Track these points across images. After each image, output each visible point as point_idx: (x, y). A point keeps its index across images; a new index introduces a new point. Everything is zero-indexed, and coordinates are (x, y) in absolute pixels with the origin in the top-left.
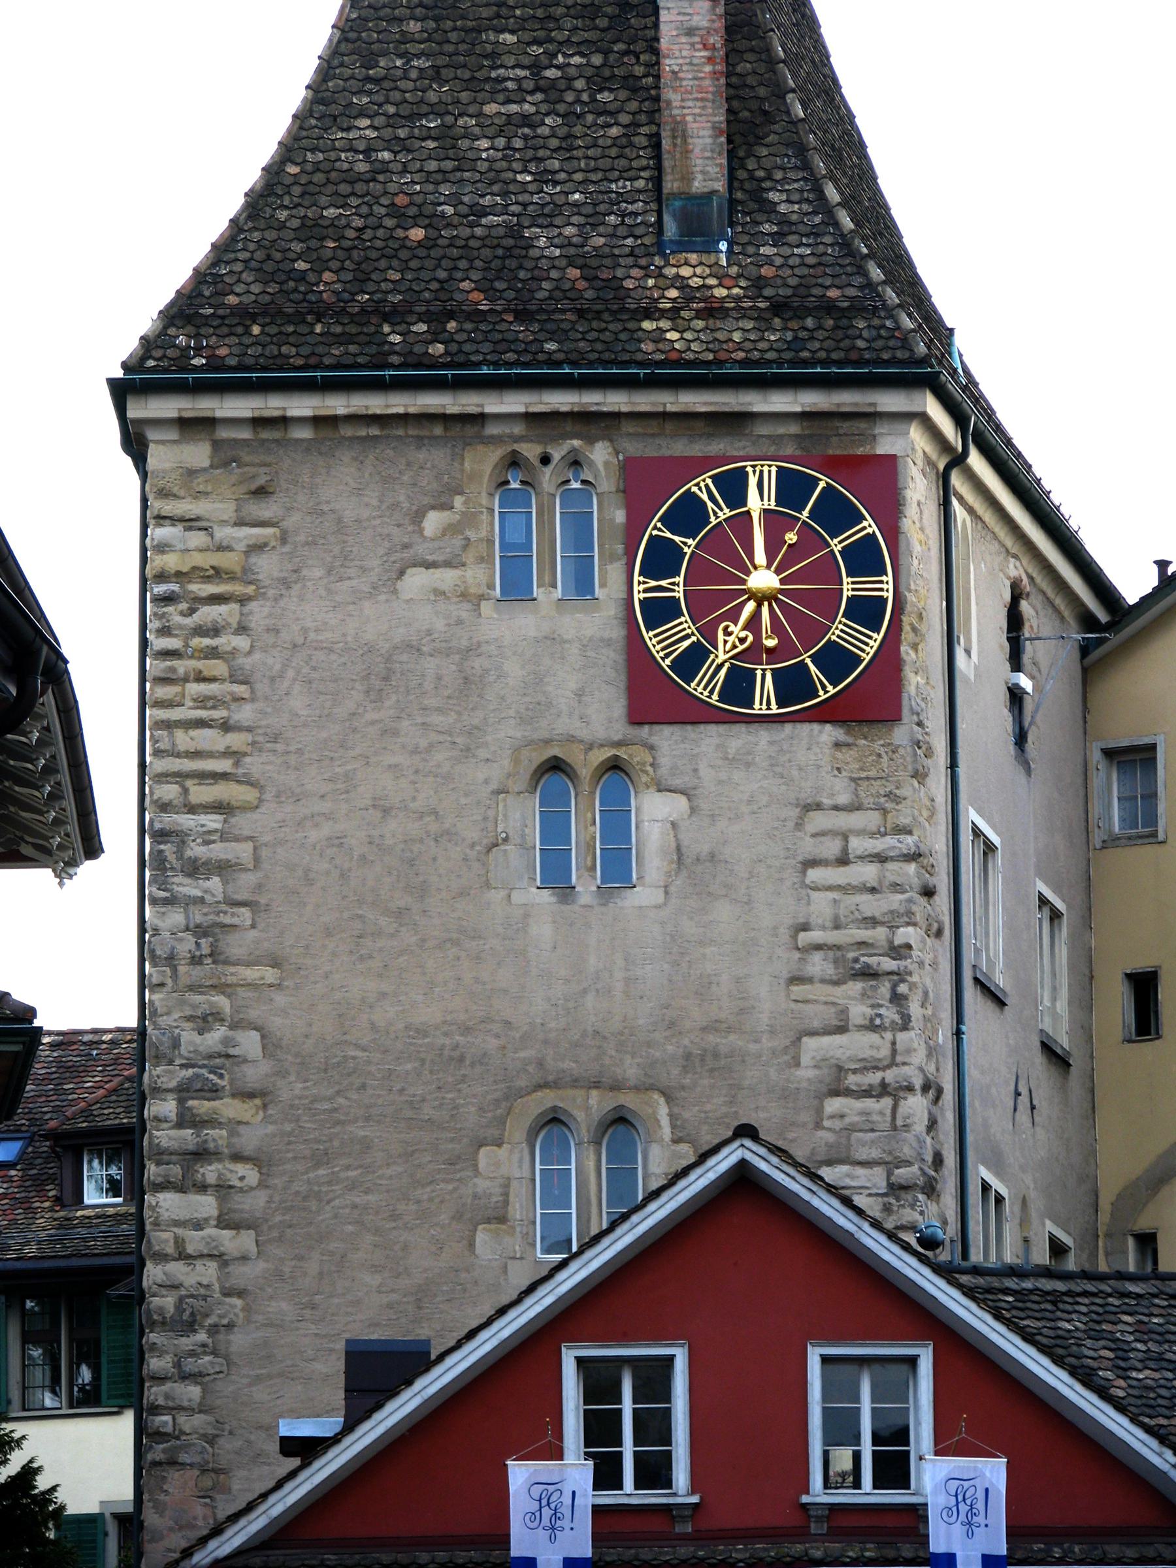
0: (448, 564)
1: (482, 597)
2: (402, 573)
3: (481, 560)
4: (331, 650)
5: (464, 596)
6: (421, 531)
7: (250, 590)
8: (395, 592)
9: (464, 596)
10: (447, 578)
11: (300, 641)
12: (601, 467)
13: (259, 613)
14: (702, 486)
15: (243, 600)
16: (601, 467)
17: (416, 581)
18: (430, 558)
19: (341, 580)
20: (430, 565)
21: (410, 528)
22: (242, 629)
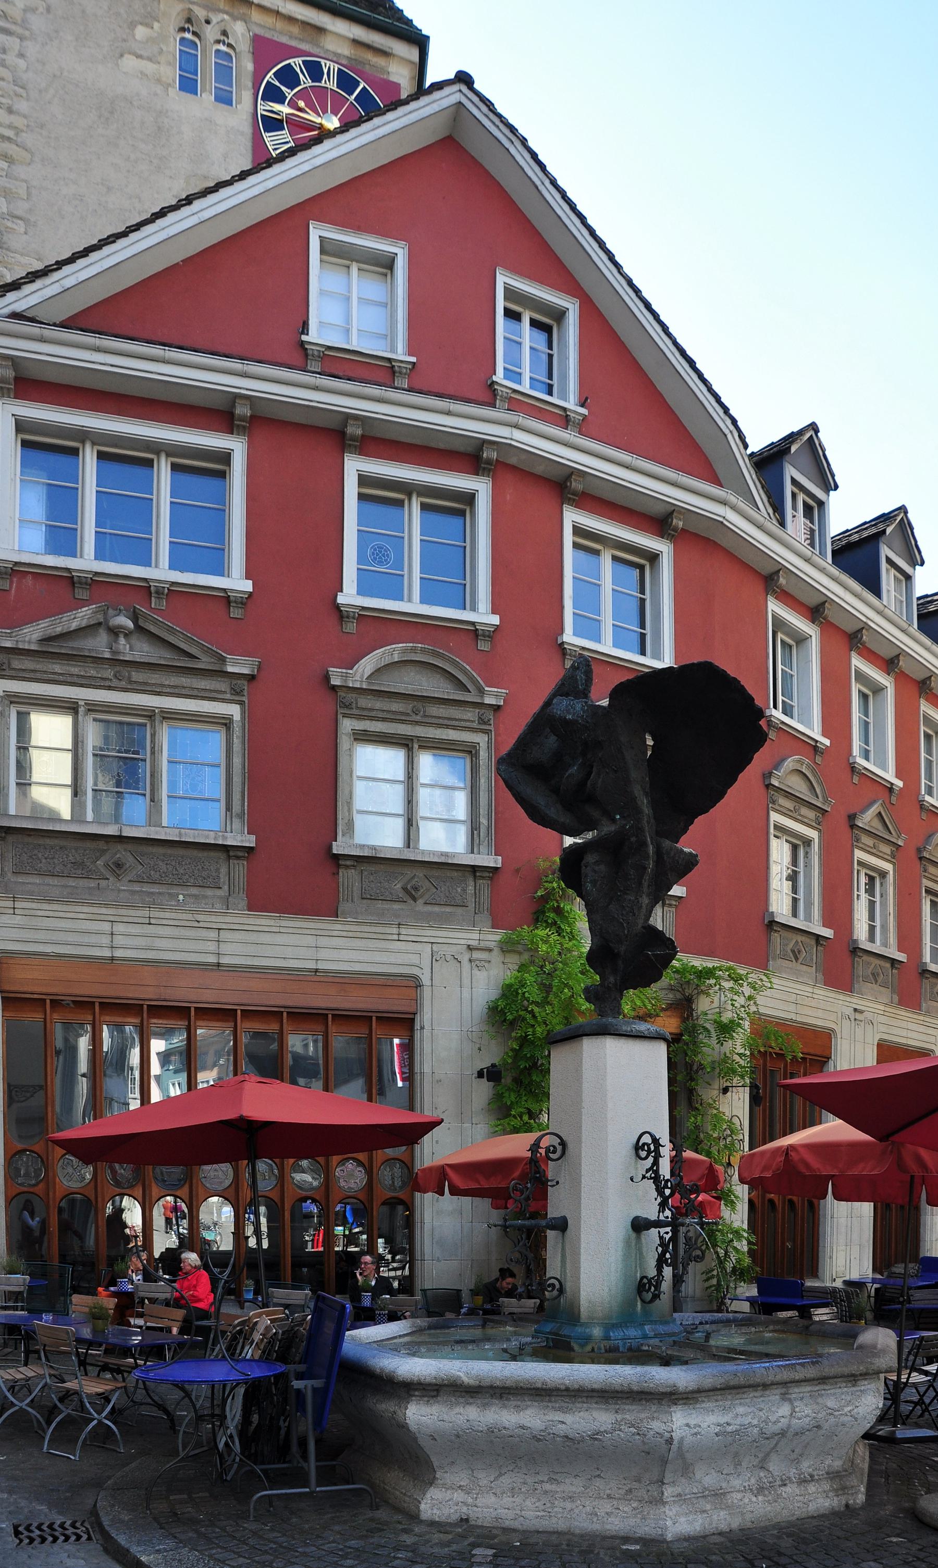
0: (150, 59)
1: (169, 85)
2: (122, 56)
3: (169, 64)
4: (77, 86)
5: (159, 81)
6: (134, 36)
7: (27, 33)
8: (117, 65)
9: (159, 81)
10: (149, 67)
11: (58, 73)
12: (240, 35)
13: (32, 49)
14: (296, 63)
15: (22, 38)
16: (240, 35)
17: (129, 62)
18: (139, 52)
19: (84, 46)
20: (139, 56)
21: (127, 31)
22: (21, 55)
